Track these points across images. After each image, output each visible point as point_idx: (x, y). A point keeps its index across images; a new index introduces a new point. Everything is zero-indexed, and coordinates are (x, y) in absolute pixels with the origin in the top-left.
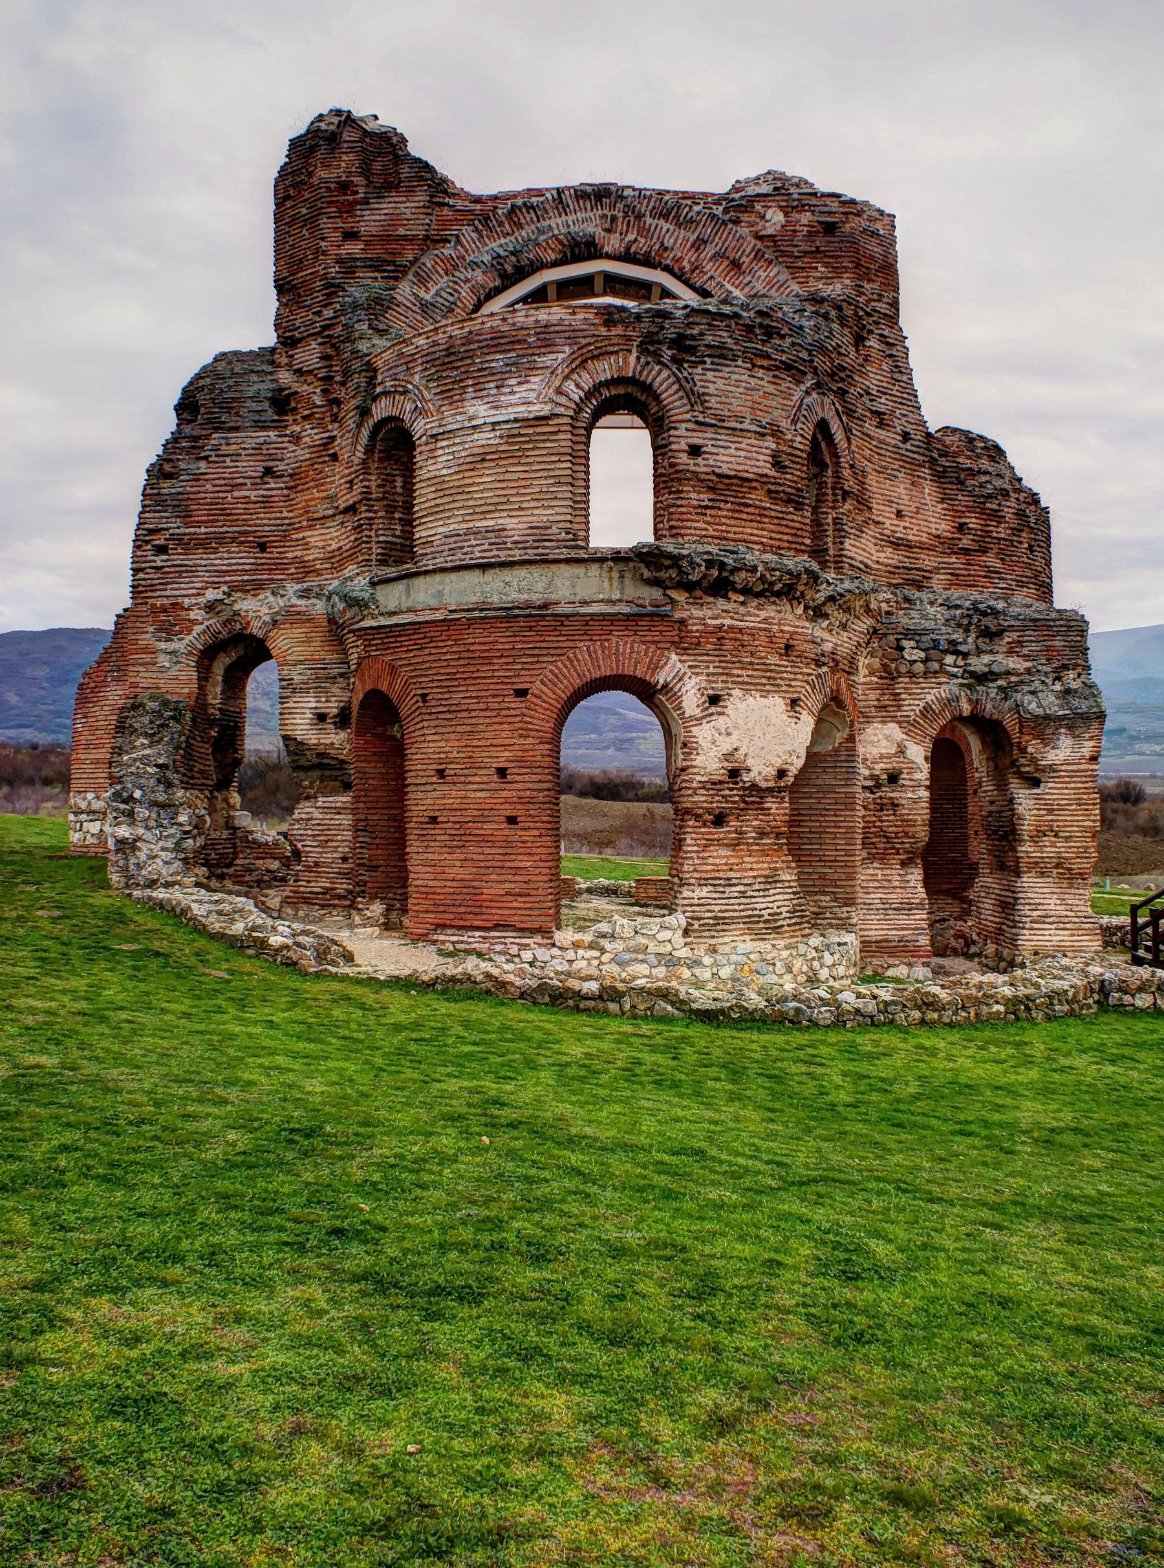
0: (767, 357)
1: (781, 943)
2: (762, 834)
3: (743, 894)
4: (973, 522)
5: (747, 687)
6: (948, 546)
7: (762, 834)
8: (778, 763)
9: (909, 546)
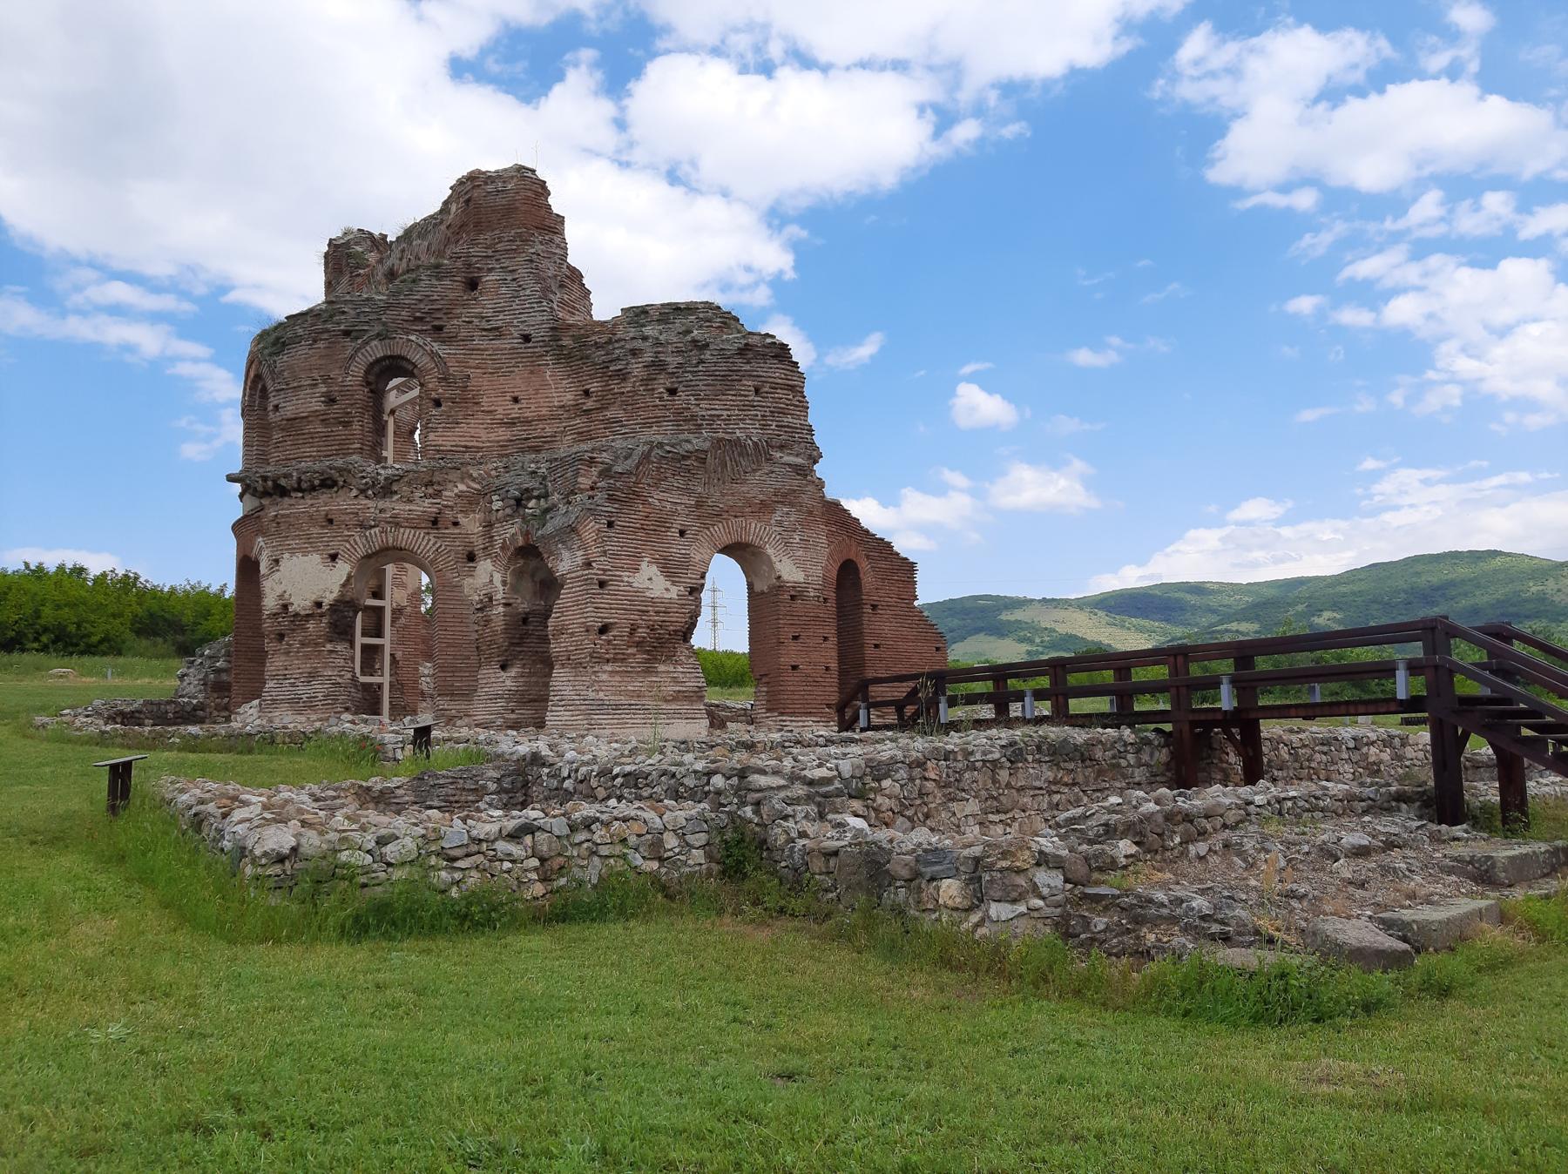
0: (327, 331)
1: (314, 717)
2: (303, 644)
3: (293, 685)
4: (594, 386)
5: (293, 552)
6: (578, 410)
7: (303, 644)
8: (314, 597)
9: (528, 422)
